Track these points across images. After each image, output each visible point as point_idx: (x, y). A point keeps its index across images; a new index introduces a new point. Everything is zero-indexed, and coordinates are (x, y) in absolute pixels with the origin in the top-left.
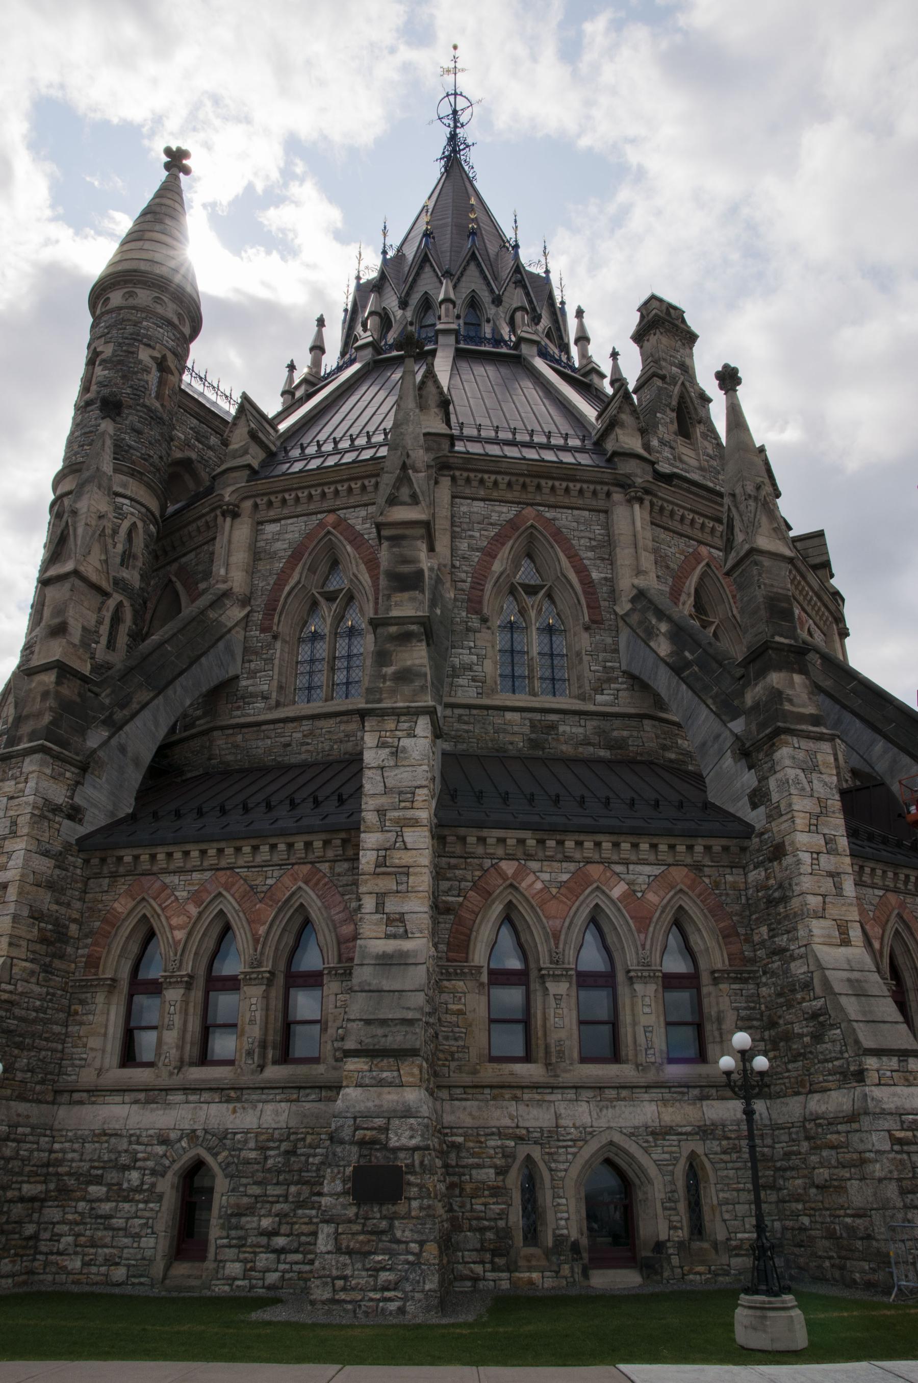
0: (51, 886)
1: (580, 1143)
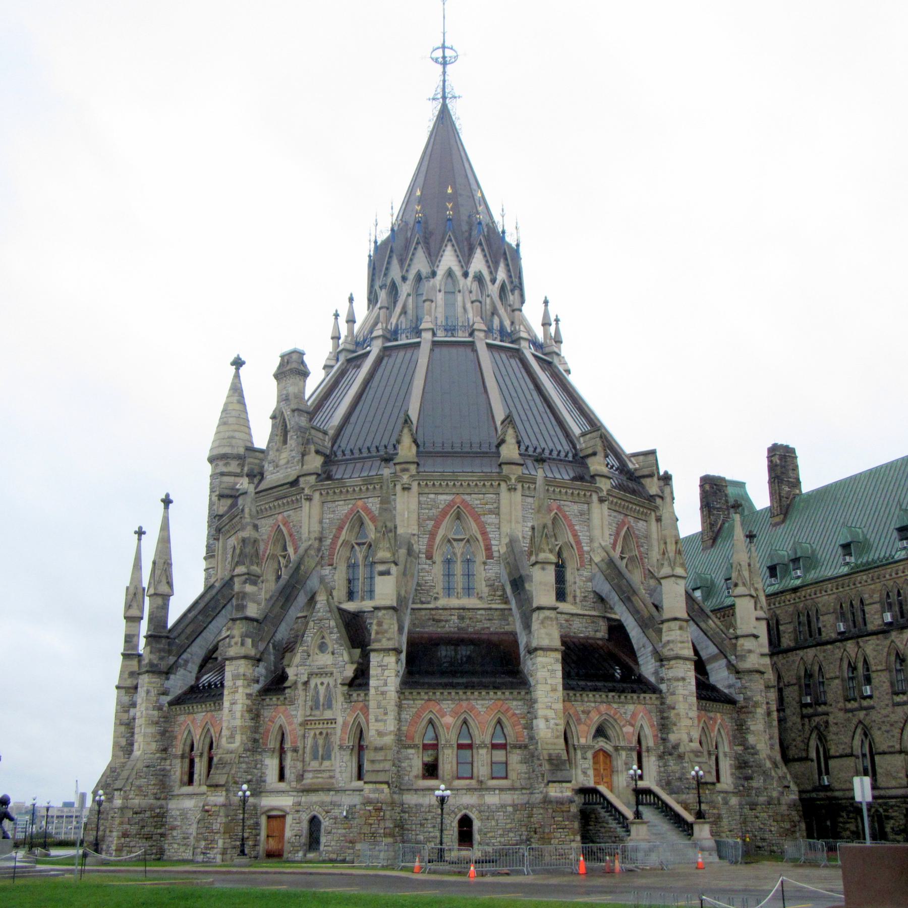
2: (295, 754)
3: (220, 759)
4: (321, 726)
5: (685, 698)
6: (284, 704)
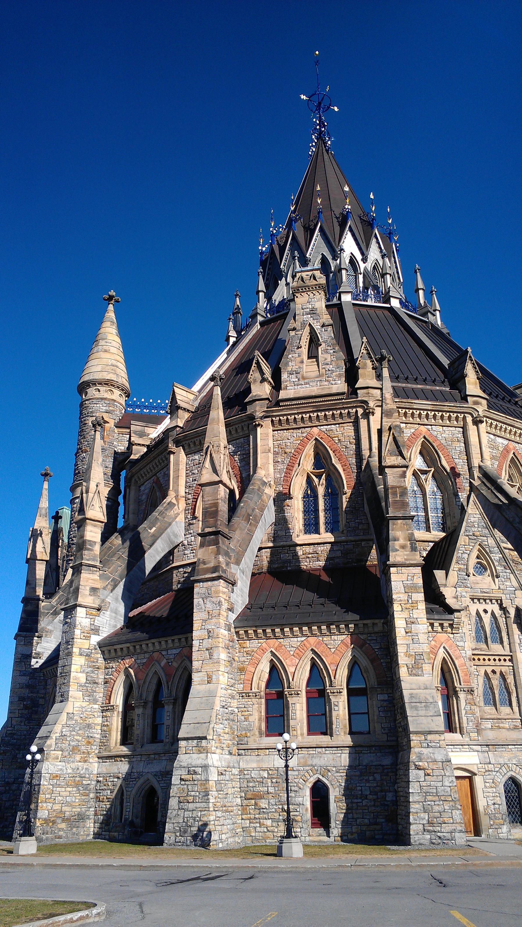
0: (28, 686)
1: (137, 780)
2: (470, 697)
3: (412, 696)
4: (492, 662)
6: (446, 632)
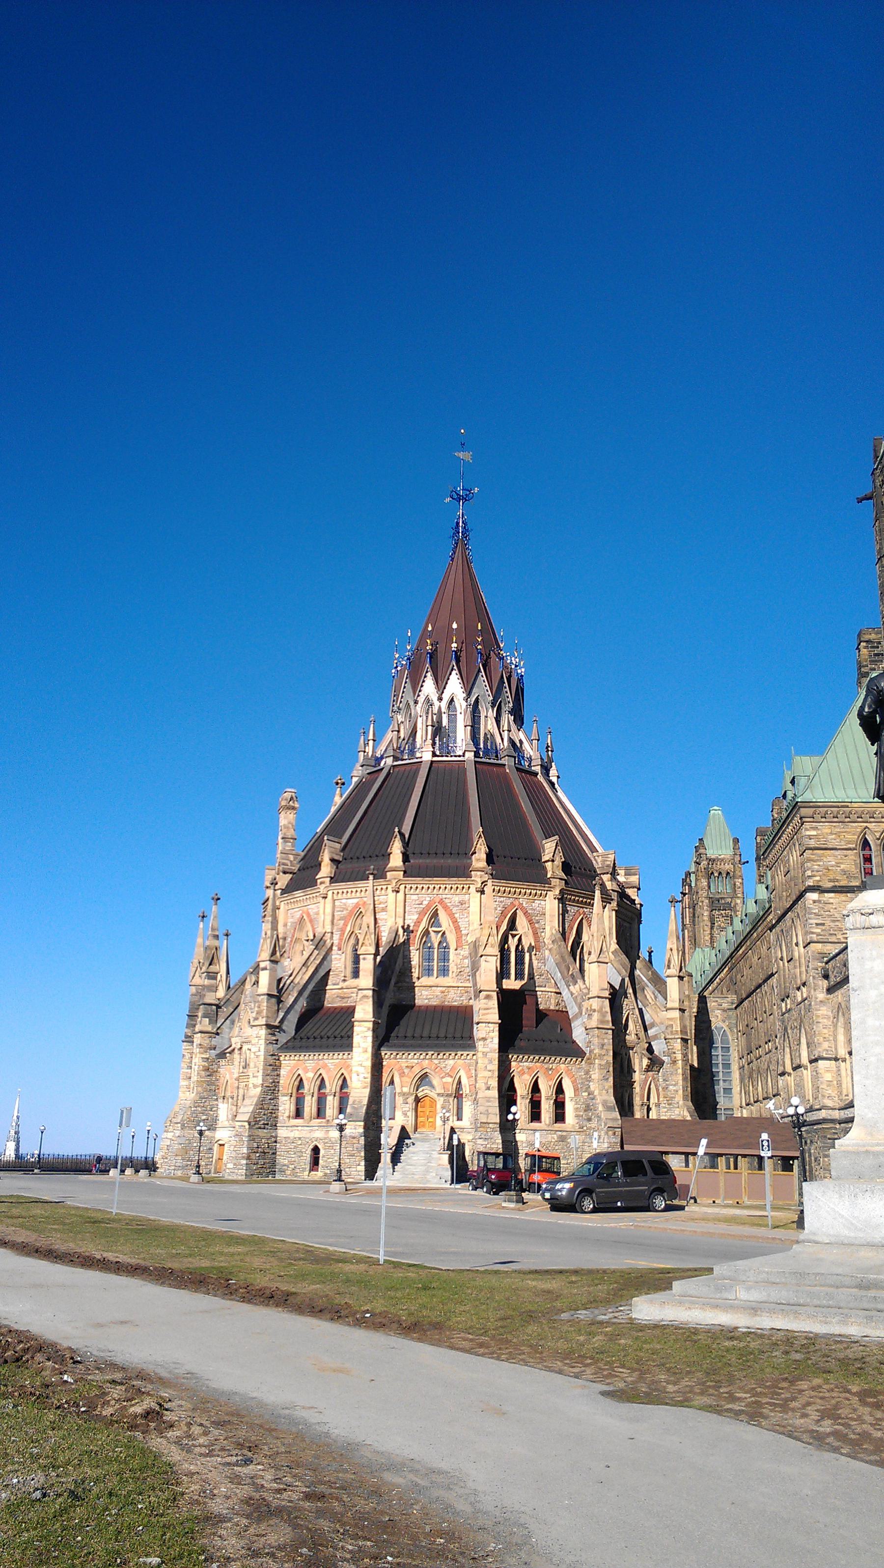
5: (485, 1054)
